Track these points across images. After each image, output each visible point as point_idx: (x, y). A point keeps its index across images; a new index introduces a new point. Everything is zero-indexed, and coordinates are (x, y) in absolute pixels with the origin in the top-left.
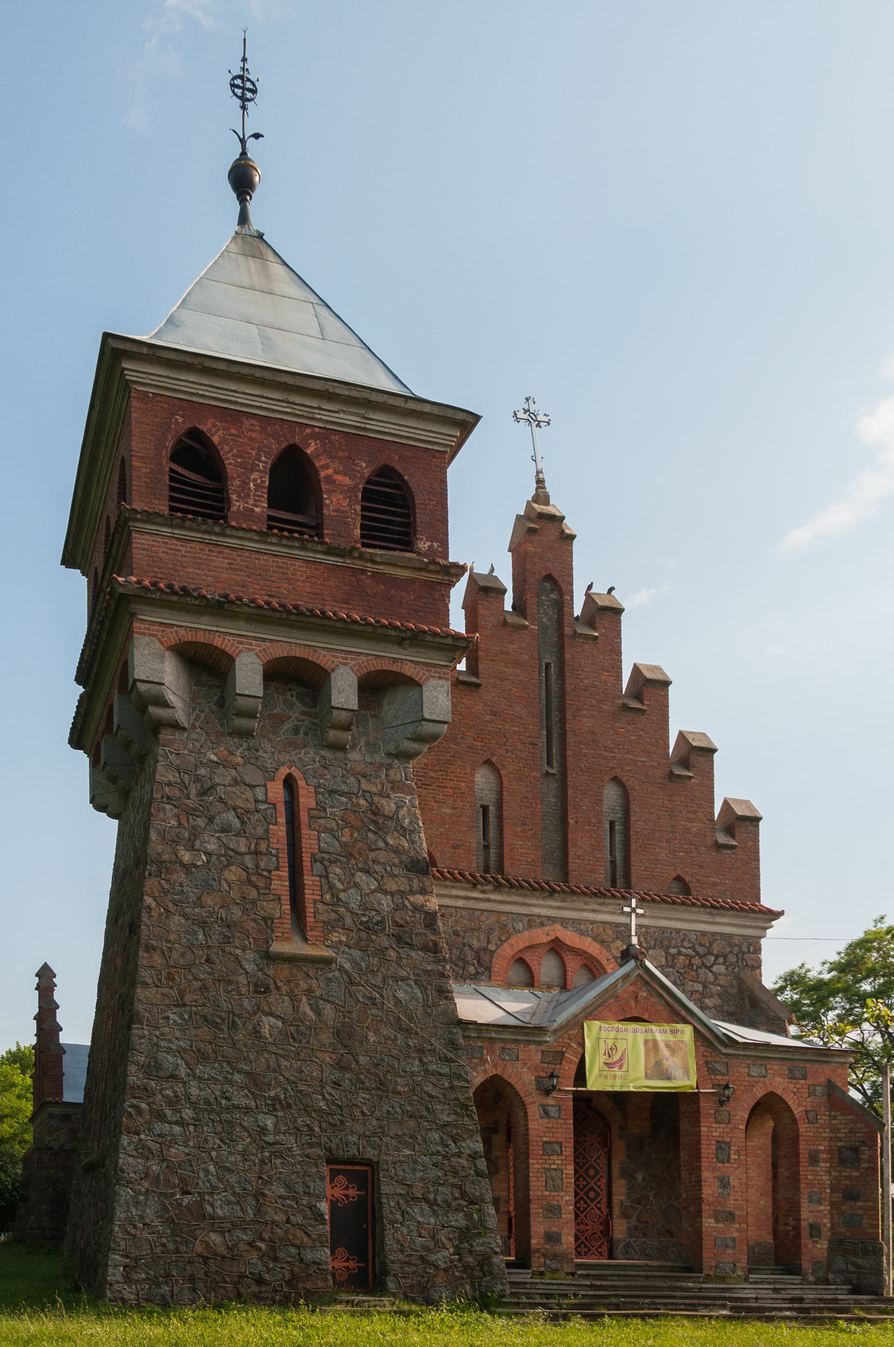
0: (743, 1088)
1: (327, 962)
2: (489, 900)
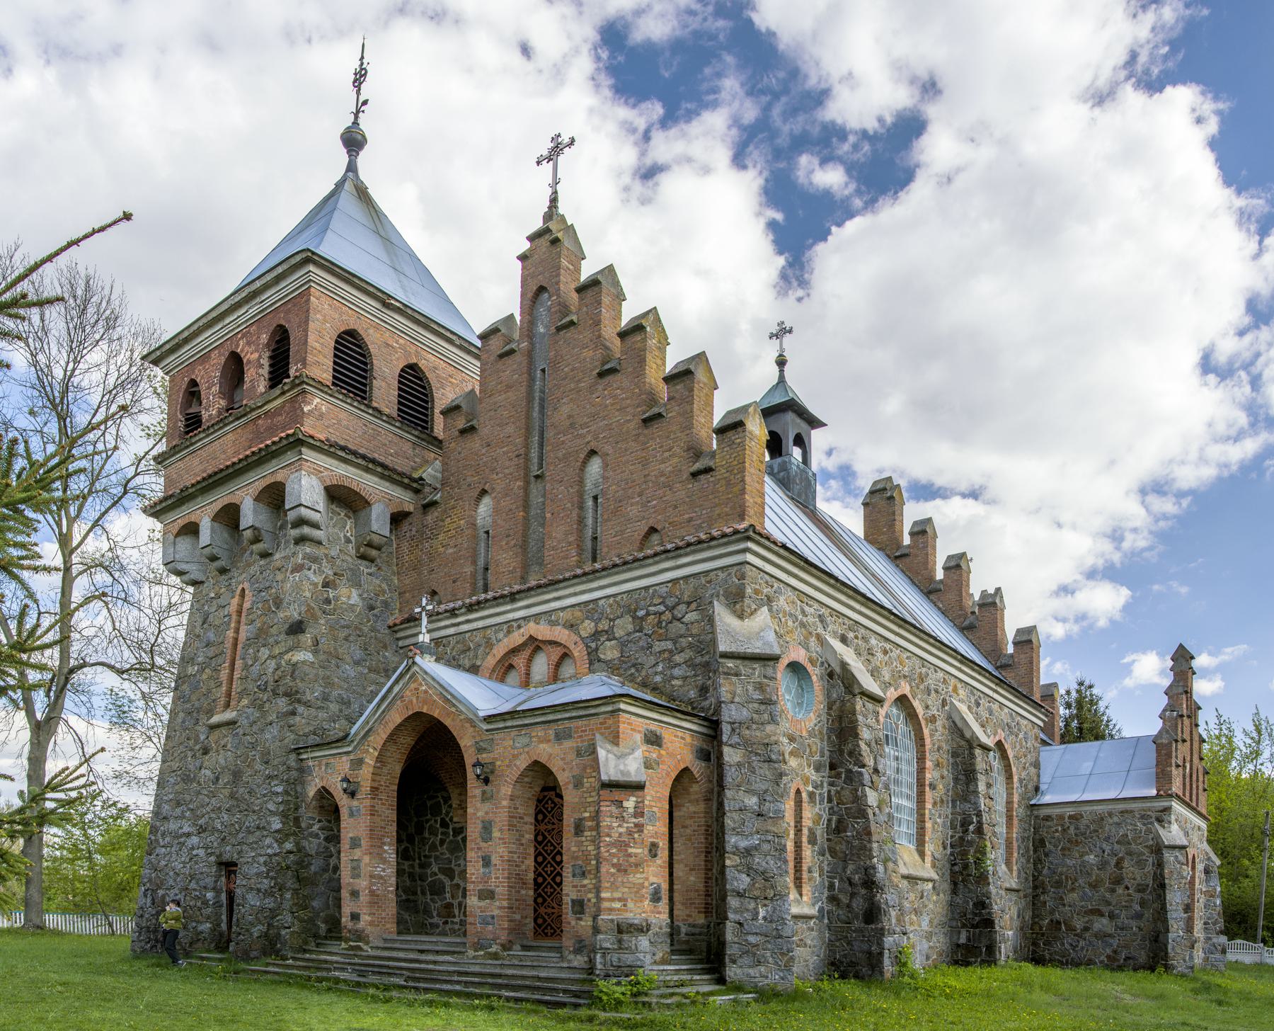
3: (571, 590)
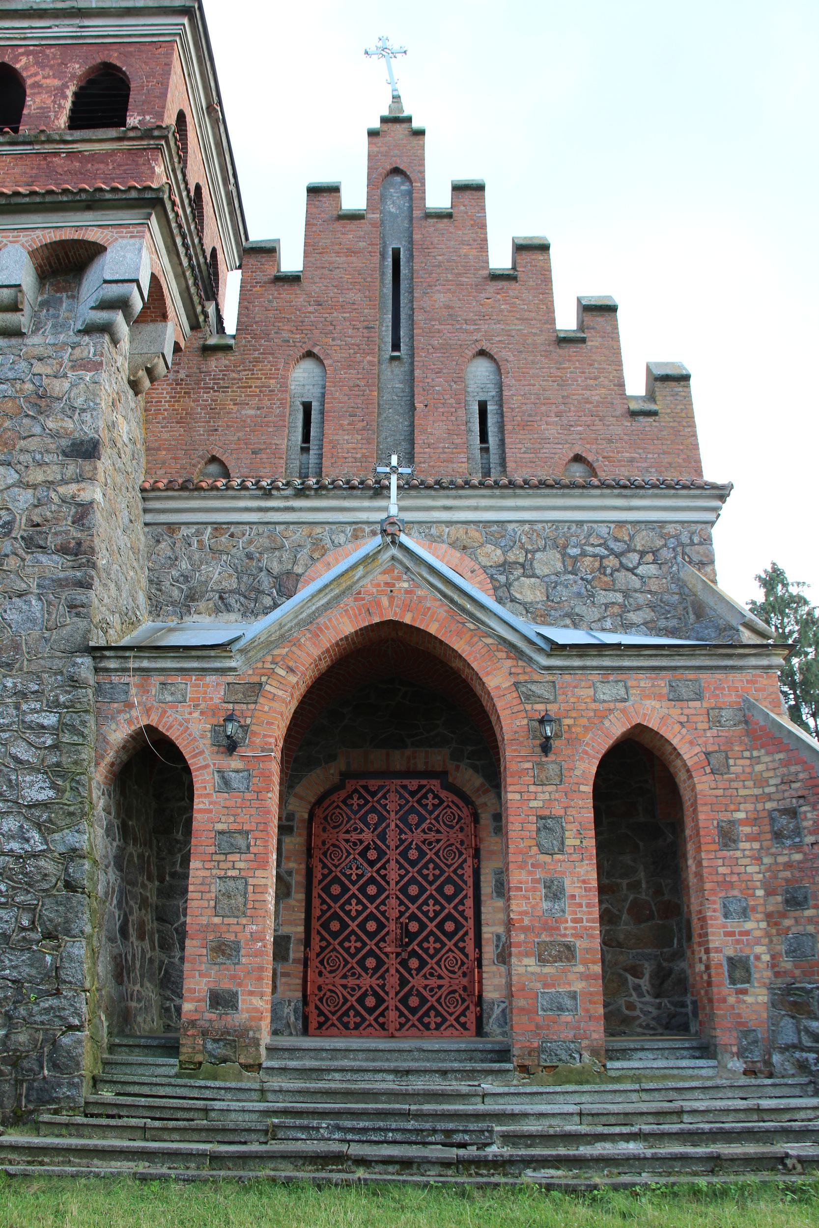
0: (584, 722)
2: (292, 509)
3: (472, 502)
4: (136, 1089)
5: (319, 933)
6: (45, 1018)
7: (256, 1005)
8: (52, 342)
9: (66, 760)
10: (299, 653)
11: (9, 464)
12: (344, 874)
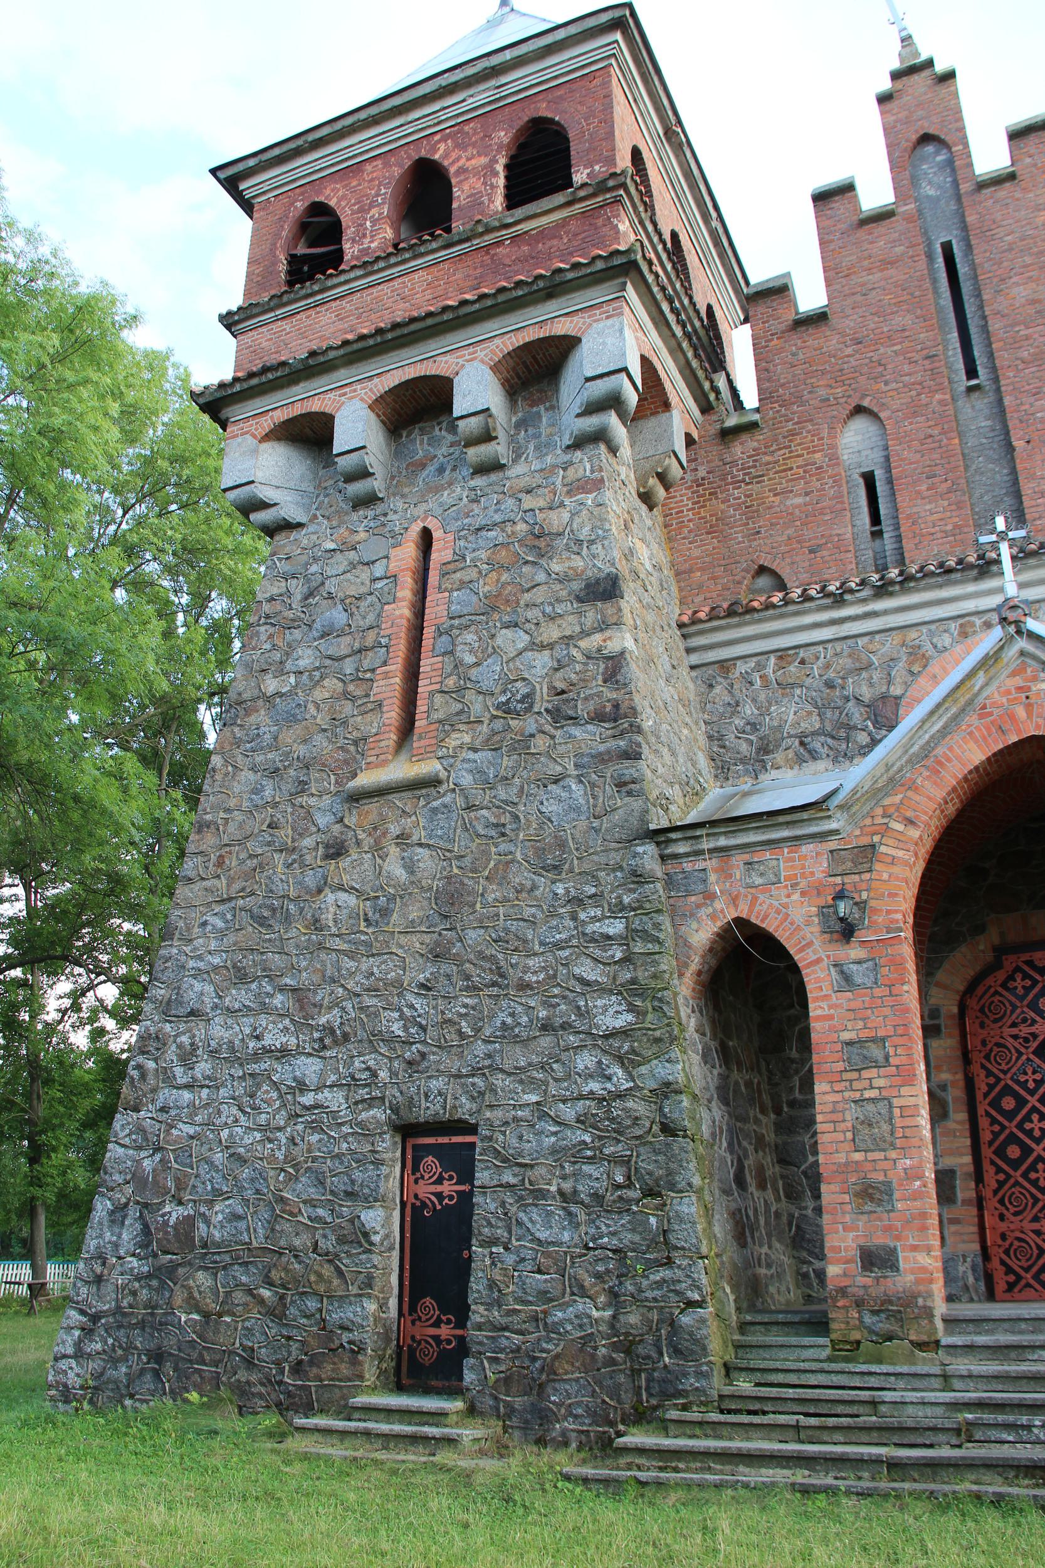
1: (432, 782)
2: (874, 614)
4: (780, 1378)
5: (992, 1163)
6: (657, 1293)
7: (924, 1262)
8: (538, 467)
9: (642, 975)
10: (918, 798)
11: (516, 625)
12: (1018, 1082)
